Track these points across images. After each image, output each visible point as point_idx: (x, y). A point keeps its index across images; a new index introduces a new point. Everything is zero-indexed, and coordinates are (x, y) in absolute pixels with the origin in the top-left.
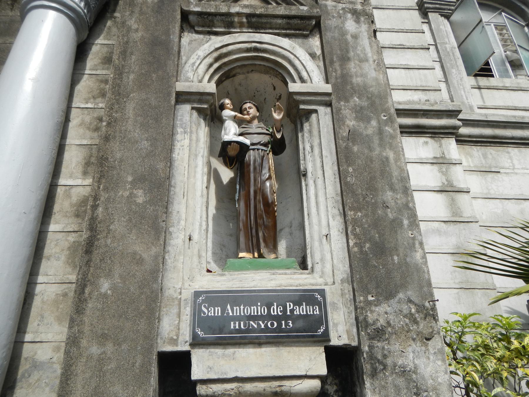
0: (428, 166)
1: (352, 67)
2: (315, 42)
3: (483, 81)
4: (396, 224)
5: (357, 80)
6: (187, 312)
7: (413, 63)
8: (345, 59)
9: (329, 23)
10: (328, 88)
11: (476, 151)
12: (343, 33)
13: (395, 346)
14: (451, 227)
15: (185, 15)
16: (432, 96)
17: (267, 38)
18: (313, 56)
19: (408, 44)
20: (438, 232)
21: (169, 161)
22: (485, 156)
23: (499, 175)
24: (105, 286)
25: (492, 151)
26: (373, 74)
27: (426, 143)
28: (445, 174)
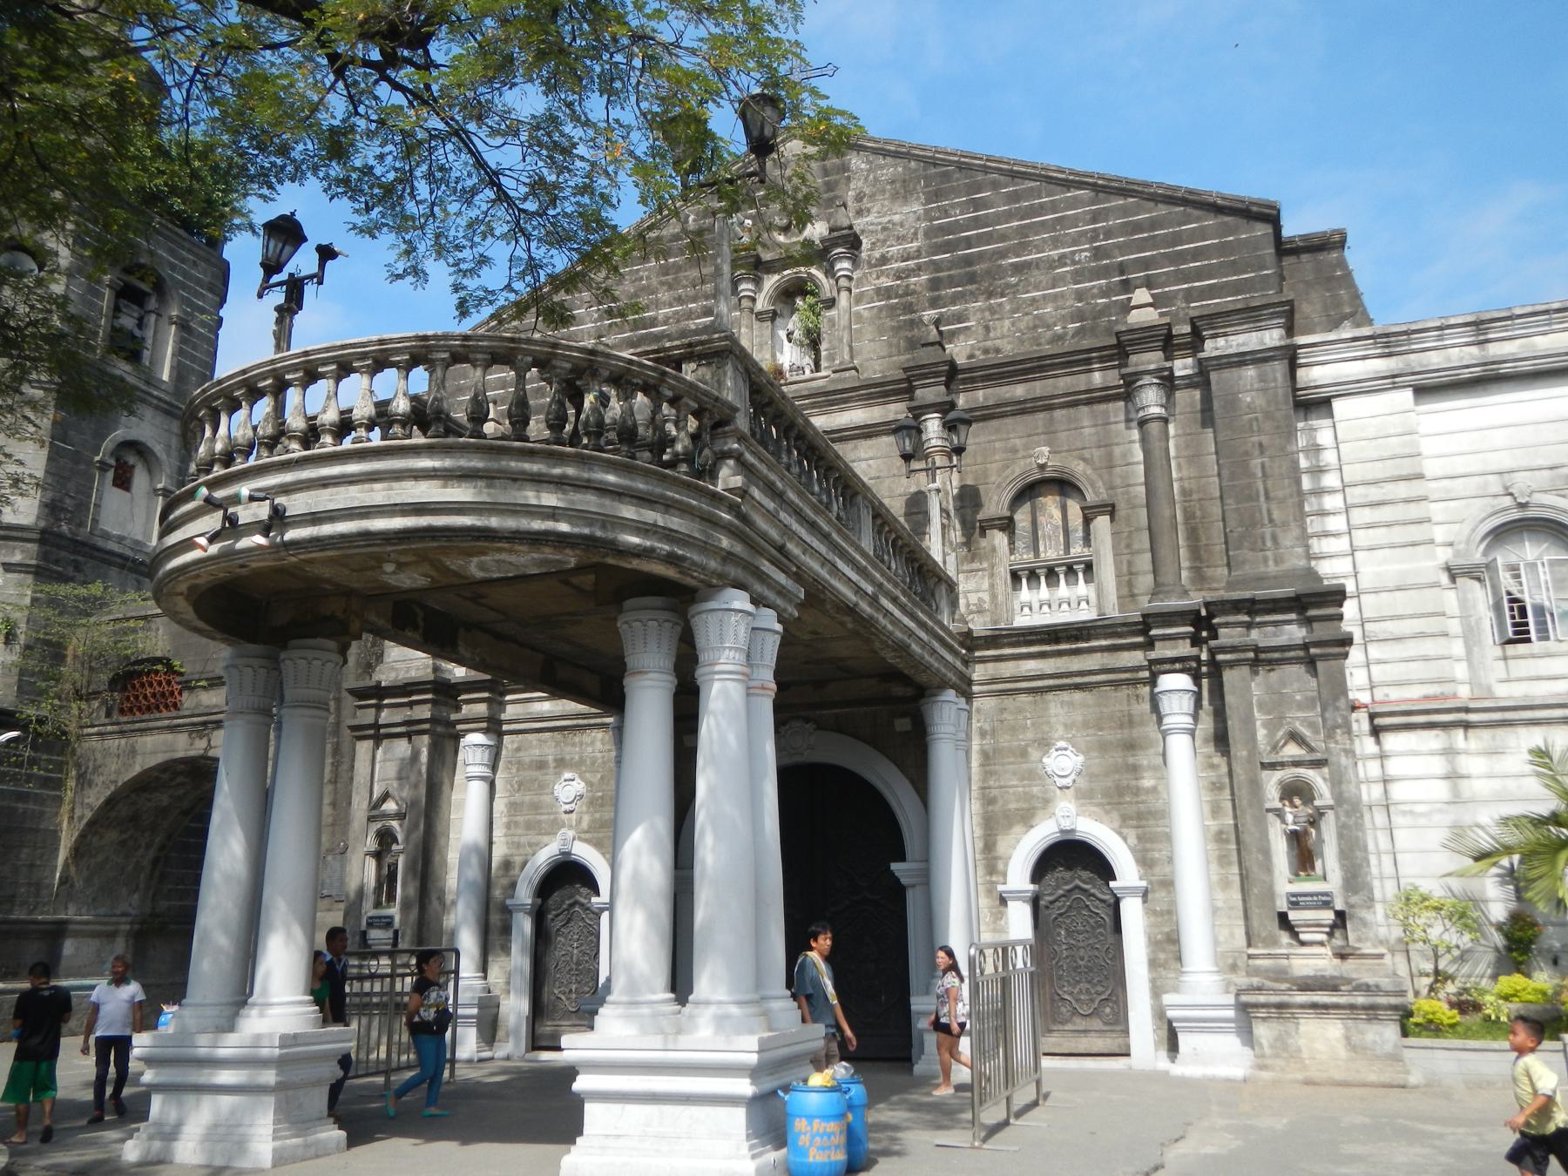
0: (1437, 757)
1: (1344, 787)
2: (1326, 770)
3: (1511, 649)
4: (1360, 866)
5: (1346, 795)
6: (1285, 900)
7: (1432, 653)
8: (1340, 783)
9: (1333, 759)
10: (1331, 802)
11: (1486, 734)
12: (1339, 765)
13: (1357, 910)
14: (1452, 807)
15: (1262, 764)
16: (1447, 689)
17: (1301, 771)
18: (1324, 779)
19: (1429, 631)
20: (1440, 811)
21: (1268, 840)
22: (1494, 738)
23: (1503, 756)
24: (1256, 891)
25: (1500, 732)
26: (1354, 790)
27: (1437, 736)
28: (1451, 762)
